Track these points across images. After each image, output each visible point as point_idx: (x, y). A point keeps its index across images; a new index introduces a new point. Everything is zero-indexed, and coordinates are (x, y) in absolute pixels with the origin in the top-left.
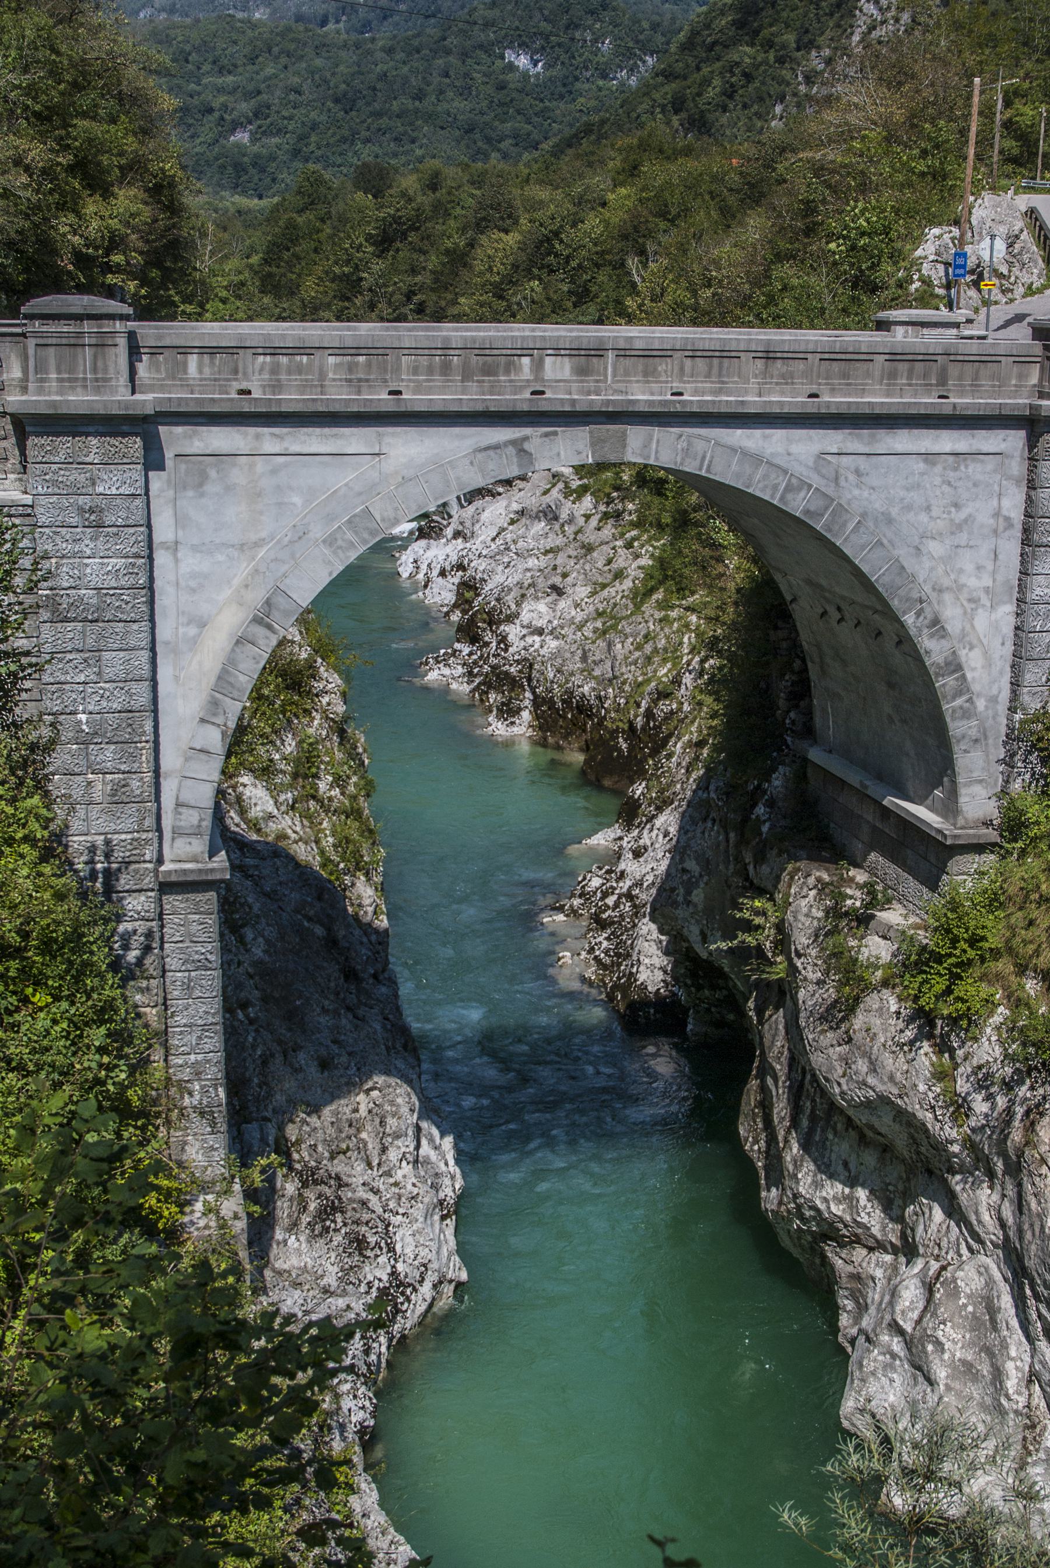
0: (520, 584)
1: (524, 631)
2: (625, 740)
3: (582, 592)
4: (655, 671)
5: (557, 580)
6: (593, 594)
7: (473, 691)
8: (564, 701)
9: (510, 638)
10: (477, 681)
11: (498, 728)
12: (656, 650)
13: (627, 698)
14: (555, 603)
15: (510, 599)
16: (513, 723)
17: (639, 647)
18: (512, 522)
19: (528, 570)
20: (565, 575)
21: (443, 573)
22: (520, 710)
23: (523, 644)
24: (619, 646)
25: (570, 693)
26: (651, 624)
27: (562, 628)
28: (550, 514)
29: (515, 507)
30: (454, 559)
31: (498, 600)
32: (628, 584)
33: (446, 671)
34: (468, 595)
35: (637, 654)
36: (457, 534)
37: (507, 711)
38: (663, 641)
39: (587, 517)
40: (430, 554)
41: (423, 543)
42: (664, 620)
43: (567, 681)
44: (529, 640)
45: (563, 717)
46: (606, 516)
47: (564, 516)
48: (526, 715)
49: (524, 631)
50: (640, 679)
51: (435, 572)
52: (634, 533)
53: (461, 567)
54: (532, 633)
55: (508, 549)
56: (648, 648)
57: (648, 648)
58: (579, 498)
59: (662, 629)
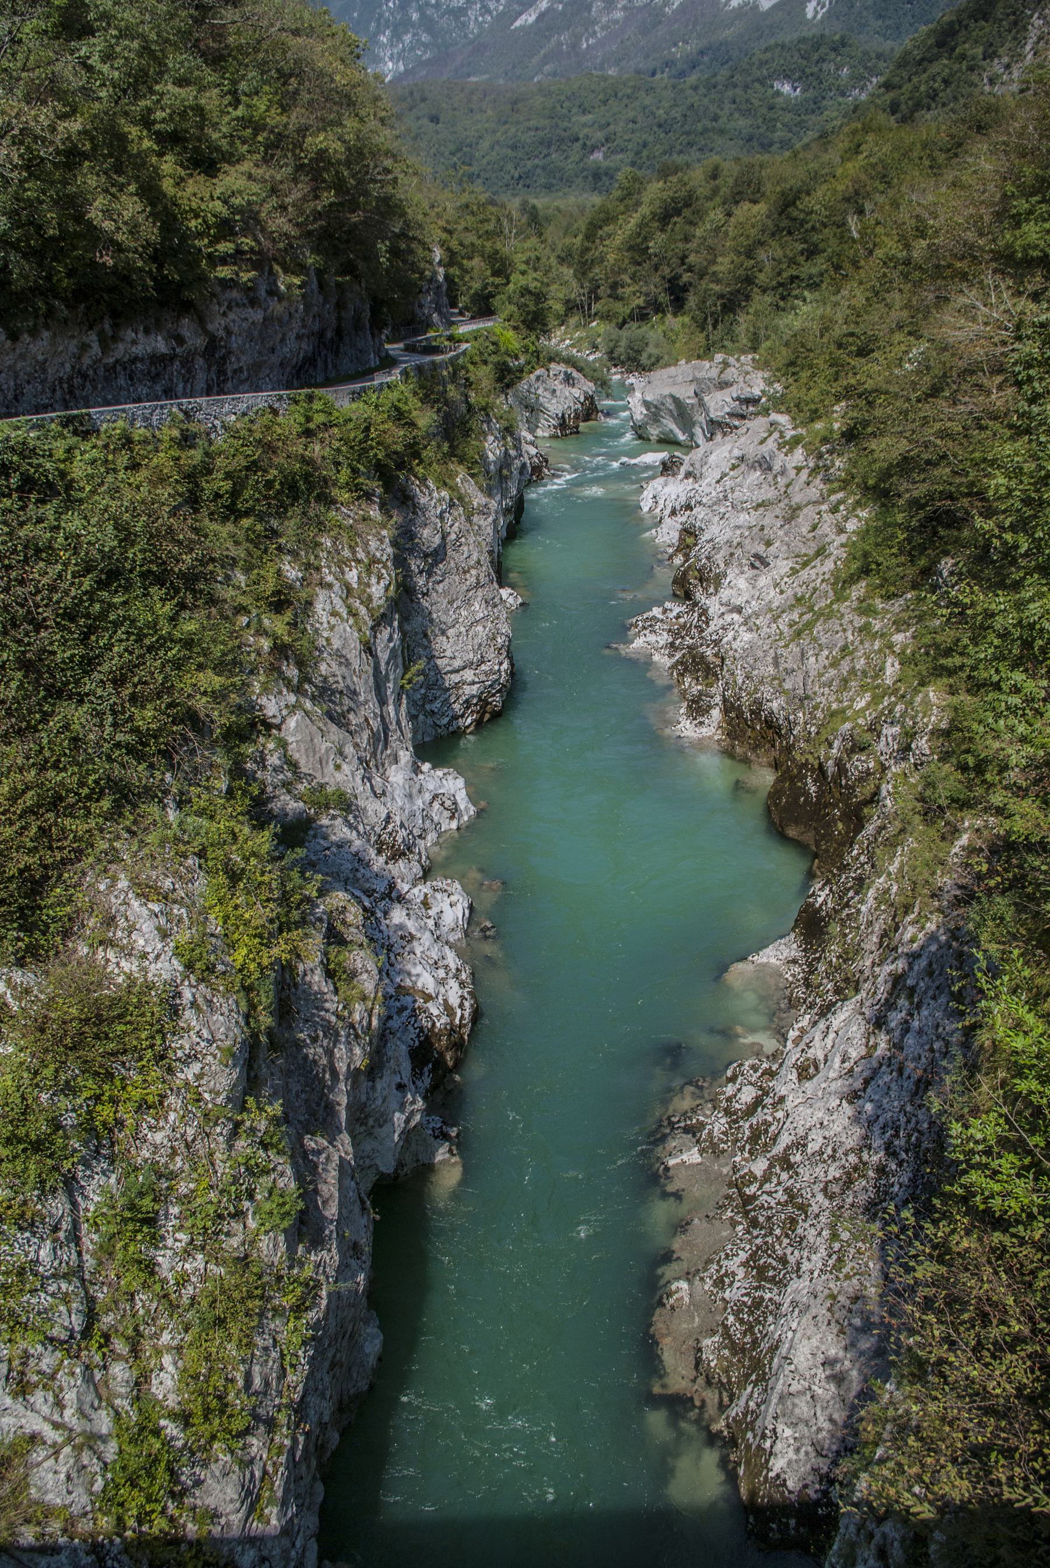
0: (729, 543)
1: (723, 609)
2: (815, 781)
3: (782, 566)
4: (852, 700)
5: (760, 549)
6: (794, 572)
7: (674, 667)
8: (752, 712)
9: (711, 611)
10: (678, 655)
11: (687, 729)
12: (853, 671)
13: (819, 727)
14: (755, 578)
15: (719, 558)
16: (701, 723)
17: (834, 664)
18: (734, 468)
19: (738, 527)
20: (769, 544)
21: (673, 513)
22: (710, 707)
23: (721, 622)
24: (812, 660)
25: (759, 703)
26: (849, 634)
27: (757, 616)
28: (764, 465)
29: (737, 453)
30: (683, 500)
31: (708, 558)
32: (829, 565)
33: (652, 638)
34: (690, 540)
35: (832, 672)
36: (688, 475)
37: (698, 709)
38: (862, 661)
39: (799, 469)
40: (667, 490)
41: (661, 480)
42: (865, 629)
43: (756, 691)
44: (728, 618)
45: (752, 729)
46: (814, 471)
47: (777, 468)
48: (716, 713)
49: (723, 609)
50: (834, 706)
51: (667, 512)
52: (840, 495)
53: (689, 507)
54: (731, 611)
55: (726, 498)
56: (845, 666)
57: (845, 666)
58: (791, 450)
59: (862, 642)
